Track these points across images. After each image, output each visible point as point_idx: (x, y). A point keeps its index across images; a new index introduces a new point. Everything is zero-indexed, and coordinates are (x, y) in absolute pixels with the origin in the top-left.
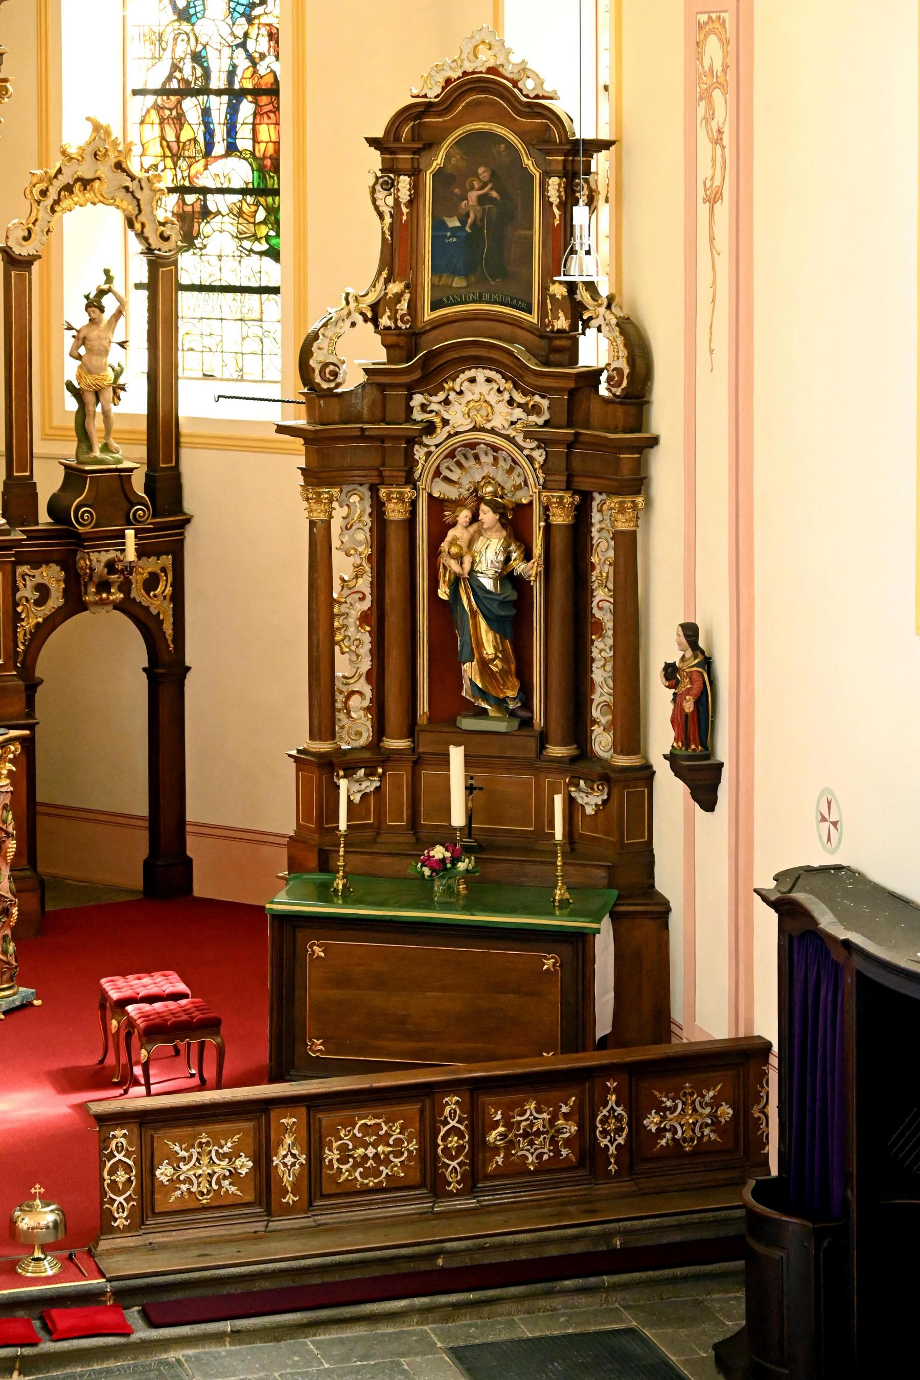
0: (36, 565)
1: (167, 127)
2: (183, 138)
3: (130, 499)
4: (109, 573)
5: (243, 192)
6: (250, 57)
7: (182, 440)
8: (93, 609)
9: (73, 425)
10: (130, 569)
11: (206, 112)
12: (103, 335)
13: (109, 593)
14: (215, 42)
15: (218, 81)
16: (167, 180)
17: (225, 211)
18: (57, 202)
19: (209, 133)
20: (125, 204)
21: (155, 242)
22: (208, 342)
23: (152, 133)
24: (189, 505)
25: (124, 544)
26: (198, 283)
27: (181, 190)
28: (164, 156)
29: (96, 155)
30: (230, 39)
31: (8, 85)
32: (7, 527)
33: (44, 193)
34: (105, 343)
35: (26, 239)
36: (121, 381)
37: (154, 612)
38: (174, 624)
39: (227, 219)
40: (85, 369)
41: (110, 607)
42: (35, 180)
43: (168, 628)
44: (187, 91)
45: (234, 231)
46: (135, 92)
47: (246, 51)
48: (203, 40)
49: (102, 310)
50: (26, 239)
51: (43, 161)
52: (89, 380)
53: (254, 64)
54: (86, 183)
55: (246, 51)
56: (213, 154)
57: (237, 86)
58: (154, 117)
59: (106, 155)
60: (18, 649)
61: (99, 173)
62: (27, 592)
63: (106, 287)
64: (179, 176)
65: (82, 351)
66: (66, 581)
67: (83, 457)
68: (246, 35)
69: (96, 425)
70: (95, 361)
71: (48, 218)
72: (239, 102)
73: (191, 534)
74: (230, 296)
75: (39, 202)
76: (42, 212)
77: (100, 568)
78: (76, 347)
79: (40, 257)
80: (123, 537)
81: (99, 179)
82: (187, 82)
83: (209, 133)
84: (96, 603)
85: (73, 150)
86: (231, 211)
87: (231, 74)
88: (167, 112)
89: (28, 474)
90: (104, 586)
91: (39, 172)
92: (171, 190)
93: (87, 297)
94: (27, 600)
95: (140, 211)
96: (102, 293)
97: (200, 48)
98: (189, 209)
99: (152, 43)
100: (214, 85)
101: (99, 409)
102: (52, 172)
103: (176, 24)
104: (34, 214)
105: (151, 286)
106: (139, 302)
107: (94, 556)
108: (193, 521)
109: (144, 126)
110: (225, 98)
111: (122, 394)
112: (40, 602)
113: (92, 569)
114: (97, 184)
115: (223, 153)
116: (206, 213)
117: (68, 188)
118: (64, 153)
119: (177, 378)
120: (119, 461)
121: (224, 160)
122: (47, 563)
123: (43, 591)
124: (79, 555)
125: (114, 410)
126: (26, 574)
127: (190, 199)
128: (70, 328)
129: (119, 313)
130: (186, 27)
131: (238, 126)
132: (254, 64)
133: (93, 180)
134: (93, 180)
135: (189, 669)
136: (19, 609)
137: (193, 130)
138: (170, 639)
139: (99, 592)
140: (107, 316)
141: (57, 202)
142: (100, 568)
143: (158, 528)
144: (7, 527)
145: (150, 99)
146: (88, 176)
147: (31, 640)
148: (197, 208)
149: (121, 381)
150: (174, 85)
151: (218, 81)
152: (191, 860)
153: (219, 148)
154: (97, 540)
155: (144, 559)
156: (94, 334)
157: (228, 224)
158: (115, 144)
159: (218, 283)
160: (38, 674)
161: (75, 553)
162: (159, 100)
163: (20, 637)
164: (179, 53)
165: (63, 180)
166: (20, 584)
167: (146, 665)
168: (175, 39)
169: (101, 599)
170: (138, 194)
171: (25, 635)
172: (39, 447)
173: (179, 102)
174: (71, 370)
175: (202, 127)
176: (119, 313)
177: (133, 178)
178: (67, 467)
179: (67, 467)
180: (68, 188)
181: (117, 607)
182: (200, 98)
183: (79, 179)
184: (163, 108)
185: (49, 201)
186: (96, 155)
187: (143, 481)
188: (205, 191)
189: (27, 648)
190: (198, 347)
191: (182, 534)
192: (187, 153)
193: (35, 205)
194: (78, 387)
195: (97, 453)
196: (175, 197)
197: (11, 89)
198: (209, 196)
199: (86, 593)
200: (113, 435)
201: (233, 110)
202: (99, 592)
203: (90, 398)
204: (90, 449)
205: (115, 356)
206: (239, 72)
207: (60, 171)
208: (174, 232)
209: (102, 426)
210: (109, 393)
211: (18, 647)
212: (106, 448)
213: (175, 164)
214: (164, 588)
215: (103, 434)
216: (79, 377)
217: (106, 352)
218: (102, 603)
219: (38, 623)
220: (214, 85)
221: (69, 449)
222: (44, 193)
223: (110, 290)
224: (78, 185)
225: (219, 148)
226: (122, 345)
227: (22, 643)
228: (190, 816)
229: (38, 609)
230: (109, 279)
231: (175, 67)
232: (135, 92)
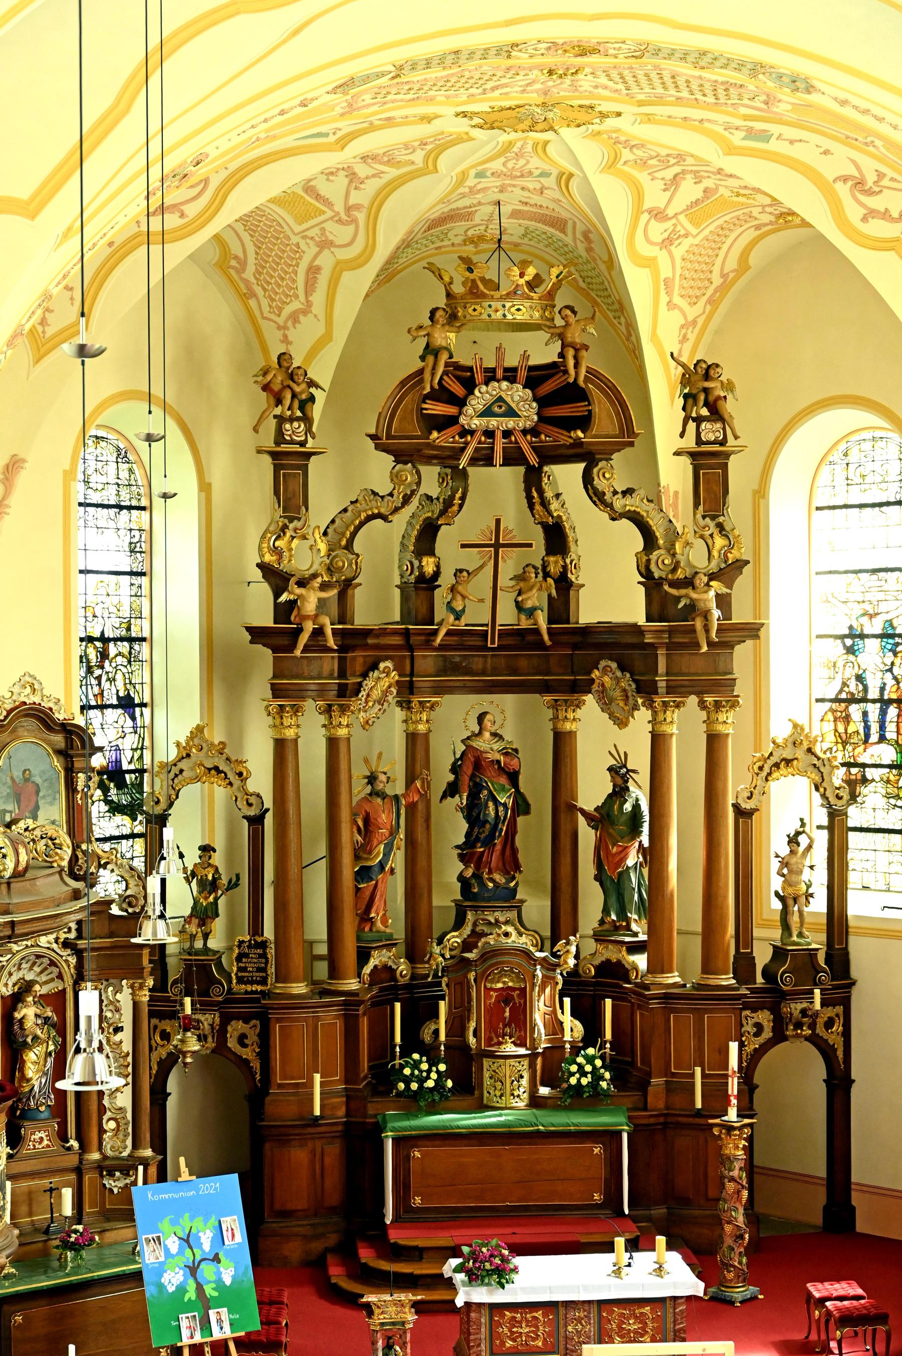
0: (754, 1010)
1: (839, 723)
2: (849, 731)
3: (817, 969)
4: (803, 1017)
5: (890, 767)
6: (895, 678)
7: (850, 930)
8: (792, 1040)
9: (778, 918)
10: (816, 1014)
11: (865, 714)
12: (799, 861)
13: (802, 1030)
14: (871, 668)
15: (873, 694)
16: (840, 757)
17: (878, 779)
18: (769, 774)
19: (867, 728)
20: (813, 776)
21: (833, 800)
22: (868, 865)
23: (829, 726)
24: (854, 973)
25: (813, 998)
26: (859, 826)
27: (848, 765)
28: (837, 743)
29: (794, 743)
30: (882, 667)
31: (739, 699)
32: (737, 985)
33: (761, 768)
34: (800, 866)
35: (749, 798)
36: (810, 891)
37: (831, 1043)
38: (844, 1051)
39: (879, 784)
40: (787, 883)
41: (803, 1039)
42: (755, 760)
43: (840, 1054)
44: (852, 700)
45: (884, 792)
46: (818, 700)
47: (893, 674)
48: (863, 667)
49: (798, 844)
50: (749, 798)
51: (757, 747)
52: (790, 890)
53: (898, 683)
54: (788, 762)
55: (893, 674)
56: (870, 741)
57: (886, 697)
58: (830, 716)
59: (801, 743)
61: (796, 756)
62: (749, 1028)
63: (801, 830)
64: (847, 756)
65: (785, 871)
66: (774, 1021)
67: (786, 941)
68: (893, 664)
69: (795, 919)
70: (794, 878)
71: (763, 784)
72: (887, 708)
73: (855, 992)
74: (882, 835)
75: (757, 774)
76: (760, 782)
77: (796, 1013)
78: (781, 869)
79: (758, 810)
80: (813, 993)
81: (796, 759)
82: (853, 694)
83: (867, 728)
84: (793, 1036)
85: (779, 741)
86: (882, 779)
87: (882, 689)
88: (839, 714)
90: (799, 1025)
91: (758, 755)
92: (843, 765)
93: (788, 836)
94: (749, 1033)
95: (823, 780)
96: (798, 833)
97: (861, 672)
98: (853, 777)
99: (829, 668)
100: (870, 696)
101: (796, 908)
102: (766, 755)
103: (845, 656)
104: (754, 782)
105: (830, 828)
106: (822, 839)
107: (792, 1006)
108: (857, 984)
109: (823, 723)
110: (878, 705)
111: (811, 899)
112: (757, 1035)
113: (791, 1014)
114: (795, 762)
115: (877, 740)
116: (865, 781)
117: (777, 765)
118: (774, 742)
119: (847, 889)
120: (809, 944)
121: (877, 746)
122: (762, 1009)
123: (759, 1027)
124: (782, 1005)
125: (806, 909)
127: (854, 771)
128: (777, 856)
129: (810, 847)
130: (851, 658)
131: (887, 723)
132: (898, 683)
133: (793, 760)
134: (793, 760)
135: (854, 1081)
136: (744, 1039)
137: (857, 725)
138: (841, 1061)
139: (795, 1029)
140: (801, 849)
141: (769, 774)
142: (796, 1013)
143: (835, 987)
144: (737, 985)
145: (828, 705)
146: (789, 757)
148: (859, 777)
149: (810, 891)
150: (844, 696)
151: (873, 694)
152: (854, 1208)
153: (874, 738)
154: (795, 995)
155: (825, 1008)
156: (793, 860)
157: (880, 788)
158: (807, 736)
159: (872, 827)
160: (756, 1081)
161: (780, 1003)
162: (834, 706)
164: (847, 676)
165: (774, 760)
166: (744, 1022)
167: (825, 1077)
168: (844, 666)
169: (797, 1034)
170: (822, 769)
172: (756, 933)
173: (847, 707)
174: (777, 883)
175: (863, 724)
176: (810, 847)
177: (819, 759)
178: (774, 946)
179: (774, 946)
180: (777, 765)
181: (807, 1039)
182: (861, 704)
183: (784, 759)
184: (836, 711)
185: (764, 774)
186: (794, 743)
187: (824, 956)
188: (864, 766)
189: (749, 1064)
190: (859, 868)
191: (850, 992)
192: (852, 741)
193: (755, 776)
194: (782, 894)
195: (795, 938)
196: (845, 769)
197: (741, 702)
198: (867, 769)
199: (787, 1030)
200: (805, 926)
201: (883, 713)
202: (795, 1029)
203: (790, 902)
204: (791, 935)
205: (806, 875)
206: (888, 688)
207: (771, 754)
208: (845, 793)
209: (798, 920)
210: (803, 899)
212: (800, 935)
213: (844, 748)
214: (838, 1028)
215: (799, 925)
216: (783, 889)
217: (802, 872)
218: (798, 1036)
219: (756, 1048)
220: (870, 696)
221: (776, 934)
222: (761, 768)
223: (804, 832)
224: (783, 763)
225: (874, 738)
226: (811, 867)
228: (854, 1178)
230: (803, 824)
231: (844, 684)
232: (818, 700)
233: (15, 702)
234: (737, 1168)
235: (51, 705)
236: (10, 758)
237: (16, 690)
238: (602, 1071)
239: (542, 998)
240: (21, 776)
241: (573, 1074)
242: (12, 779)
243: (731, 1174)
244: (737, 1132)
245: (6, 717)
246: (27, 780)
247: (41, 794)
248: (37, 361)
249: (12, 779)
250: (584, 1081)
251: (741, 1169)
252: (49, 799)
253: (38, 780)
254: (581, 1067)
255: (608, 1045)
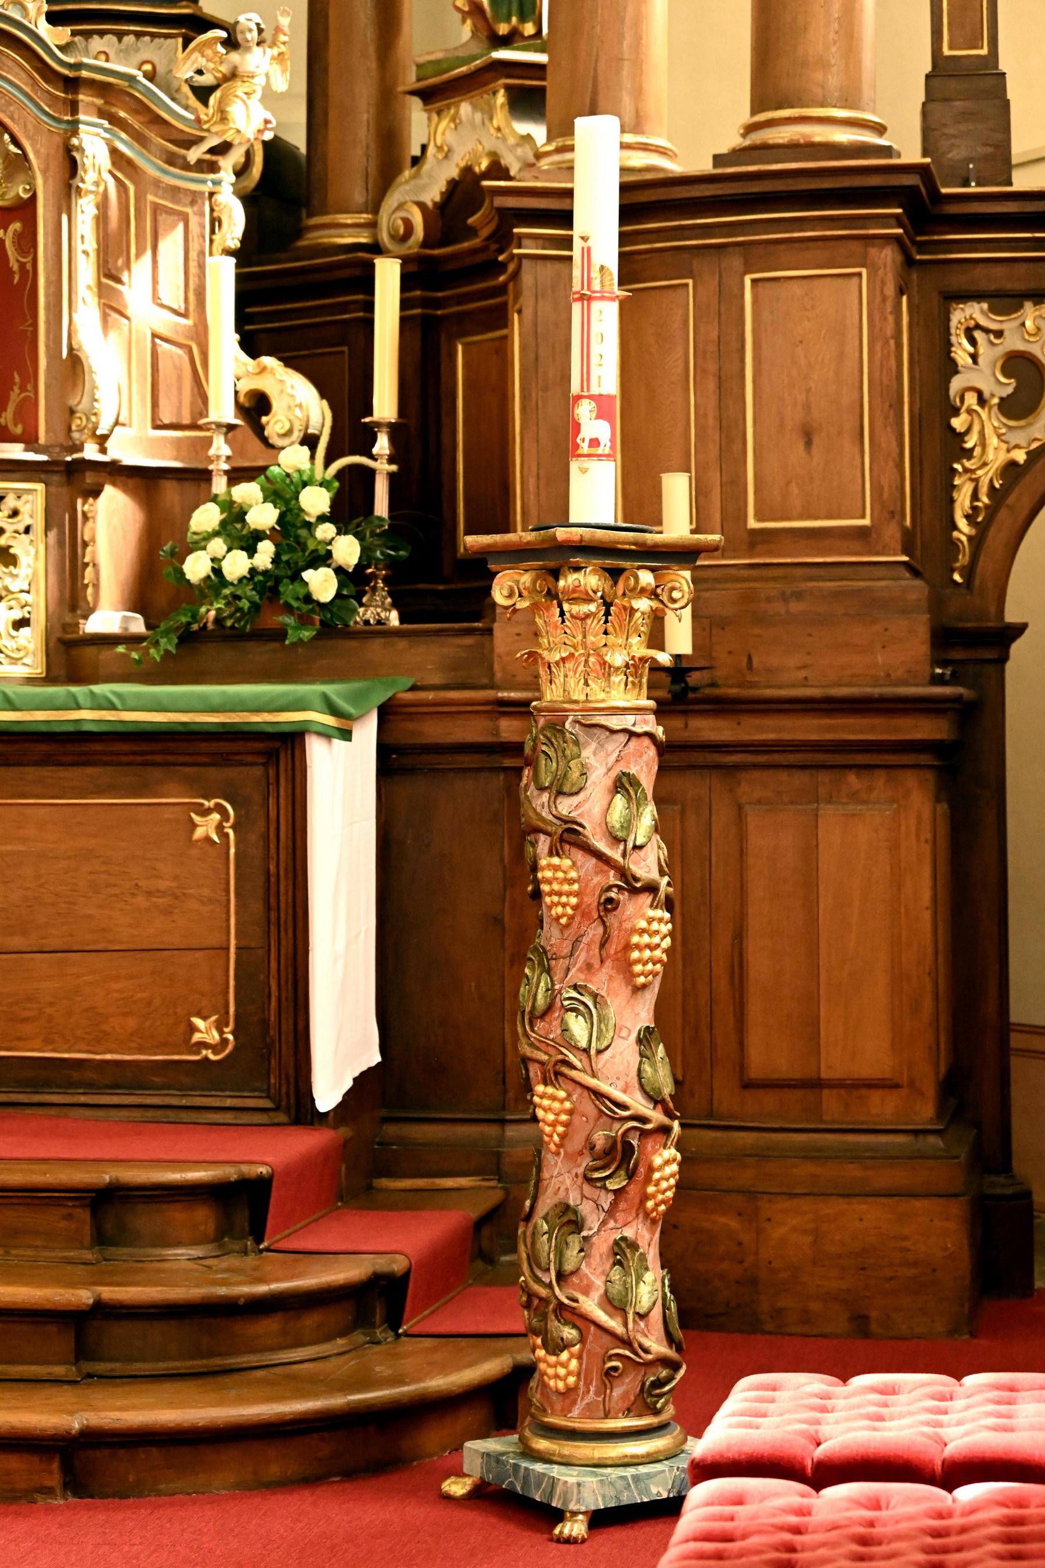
60: (955, 534)
89: (984, 51)
126: (978, 327)
136: (958, 423)
147: (992, 511)
163: (963, 501)
171: (975, 496)
211: (955, 527)
219: (1013, 464)
227: (967, 517)
229: (1011, 423)
234: (599, 779)
238: (327, 531)
239: (141, 267)
241: (200, 543)
243: (565, 806)
244: (590, 579)
250: (236, 565)
251: (624, 784)
254: (235, 514)
255: (382, 444)
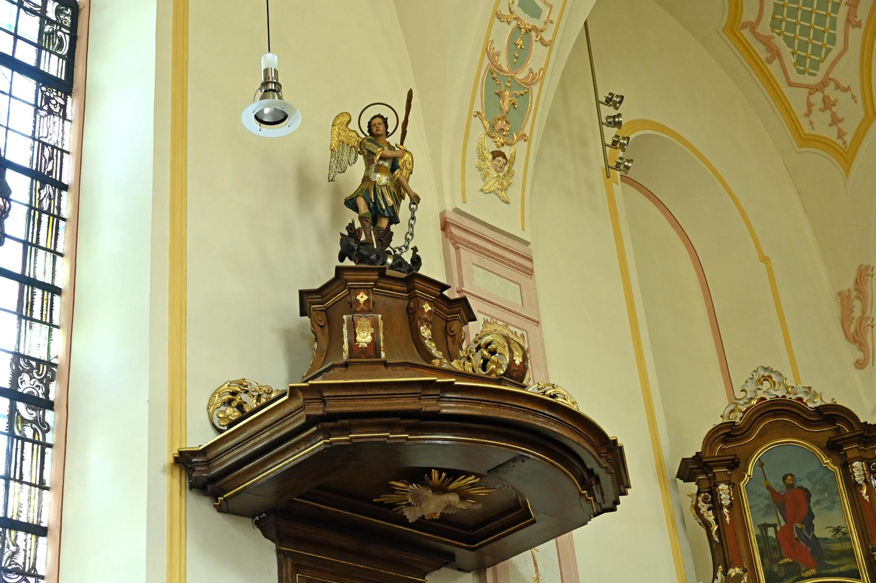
233: (752, 399)
235: (799, 395)
236: (762, 465)
237: (751, 387)
240: (782, 483)
242: (769, 487)
245: (741, 418)
246: (790, 487)
247: (813, 500)
248: (847, 173)
249: (769, 487)
252: (826, 504)
253: (806, 484)
